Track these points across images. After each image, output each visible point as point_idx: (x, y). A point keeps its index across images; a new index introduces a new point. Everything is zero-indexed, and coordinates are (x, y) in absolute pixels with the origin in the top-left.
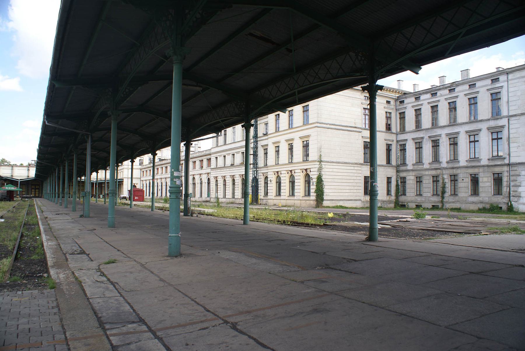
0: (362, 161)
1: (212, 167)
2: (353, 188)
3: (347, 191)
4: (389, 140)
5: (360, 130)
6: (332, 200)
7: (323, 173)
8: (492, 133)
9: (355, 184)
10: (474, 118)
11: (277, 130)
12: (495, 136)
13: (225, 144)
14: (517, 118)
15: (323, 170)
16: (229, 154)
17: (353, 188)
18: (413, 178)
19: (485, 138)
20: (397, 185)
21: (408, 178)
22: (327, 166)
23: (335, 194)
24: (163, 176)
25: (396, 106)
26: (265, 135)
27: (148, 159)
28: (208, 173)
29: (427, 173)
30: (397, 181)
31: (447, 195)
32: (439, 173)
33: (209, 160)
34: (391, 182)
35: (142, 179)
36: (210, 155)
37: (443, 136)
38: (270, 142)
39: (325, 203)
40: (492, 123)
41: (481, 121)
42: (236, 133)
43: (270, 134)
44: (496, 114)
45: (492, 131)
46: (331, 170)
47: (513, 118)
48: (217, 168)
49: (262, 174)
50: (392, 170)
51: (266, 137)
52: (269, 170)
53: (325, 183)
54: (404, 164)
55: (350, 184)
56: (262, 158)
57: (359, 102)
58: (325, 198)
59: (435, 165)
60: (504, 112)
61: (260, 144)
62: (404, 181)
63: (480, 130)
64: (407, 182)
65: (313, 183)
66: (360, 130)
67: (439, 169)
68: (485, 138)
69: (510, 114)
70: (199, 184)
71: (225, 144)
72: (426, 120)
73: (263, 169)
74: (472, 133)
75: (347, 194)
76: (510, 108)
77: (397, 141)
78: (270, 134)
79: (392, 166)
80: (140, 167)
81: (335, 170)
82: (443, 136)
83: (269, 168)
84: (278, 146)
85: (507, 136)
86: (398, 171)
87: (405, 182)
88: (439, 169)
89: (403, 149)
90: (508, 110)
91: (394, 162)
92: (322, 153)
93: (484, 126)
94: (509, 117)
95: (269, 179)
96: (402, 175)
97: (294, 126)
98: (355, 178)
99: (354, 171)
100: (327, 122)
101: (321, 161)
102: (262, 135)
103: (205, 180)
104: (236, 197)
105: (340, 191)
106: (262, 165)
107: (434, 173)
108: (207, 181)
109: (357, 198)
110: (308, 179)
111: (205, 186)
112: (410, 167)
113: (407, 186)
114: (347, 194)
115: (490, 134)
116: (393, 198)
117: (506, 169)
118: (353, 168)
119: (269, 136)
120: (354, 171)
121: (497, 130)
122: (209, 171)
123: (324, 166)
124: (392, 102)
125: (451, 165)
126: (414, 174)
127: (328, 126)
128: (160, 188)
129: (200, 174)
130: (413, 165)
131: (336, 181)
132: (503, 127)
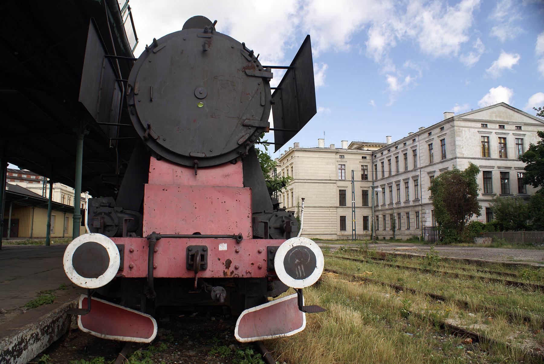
0: (338, 205)
2: (328, 225)
3: (323, 227)
4: (365, 187)
5: (335, 182)
9: (330, 222)
17: (328, 225)
23: (312, 230)
25: (372, 160)
31: (396, 229)
37: (394, 183)
46: (308, 213)
50: (369, 211)
57: (334, 161)
66: (335, 182)
75: (323, 230)
98: (331, 218)
101: (299, 207)
109: (333, 233)
114: (323, 230)
116: (370, 232)
117: (420, 208)
124: (368, 157)
127: (305, 181)
131: (313, 220)
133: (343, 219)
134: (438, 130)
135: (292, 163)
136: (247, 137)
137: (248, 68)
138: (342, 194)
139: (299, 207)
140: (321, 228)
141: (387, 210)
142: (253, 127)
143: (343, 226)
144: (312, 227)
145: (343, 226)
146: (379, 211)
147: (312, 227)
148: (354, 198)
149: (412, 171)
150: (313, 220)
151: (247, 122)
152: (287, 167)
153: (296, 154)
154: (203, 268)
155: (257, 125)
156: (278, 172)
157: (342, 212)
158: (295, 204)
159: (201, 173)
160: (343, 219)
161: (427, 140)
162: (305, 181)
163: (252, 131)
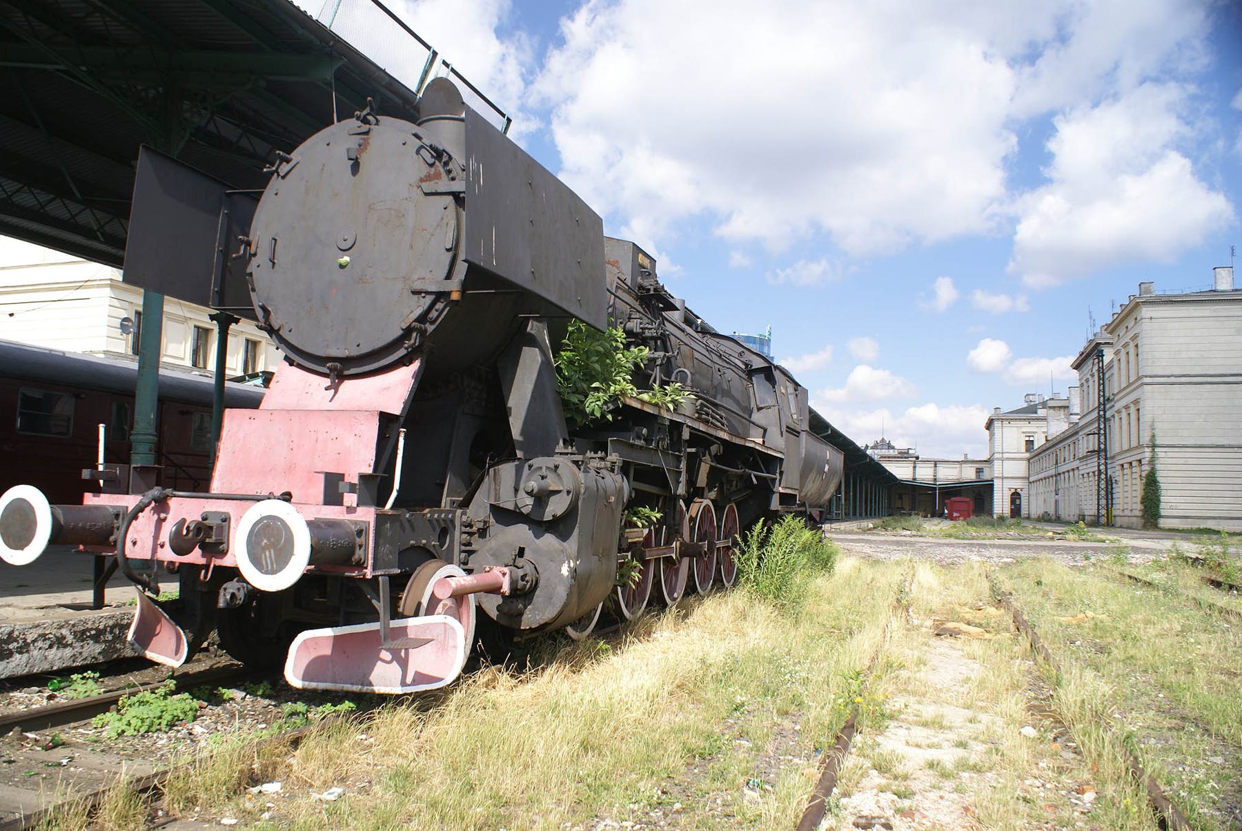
3: (1227, 500)
6: (1187, 517)
7: (1158, 467)
15: (1162, 461)
35: (1031, 479)
36: (1077, 433)
39: (1163, 523)
46: (1182, 461)
58: (1163, 512)
80: (1027, 455)
81: (1191, 461)
92: (1156, 432)
100: (1168, 373)
101: (1154, 446)
105: (1207, 500)
123: (1161, 455)
127: (1172, 380)
131: (1196, 480)
135: (1135, 337)
136: (418, 312)
137: (428, 178)
139: (1154, 446)
140: (1220, 501)
142: (427, 293)
144: (1195, 500)
147: (1195, 500)
150: (1196, 480)
151: (418, 286)
152: (1126, 345)
153: (1146, 312)
154: (224, 553)
155: (434, 289)
156: (1106, 359)
158: (1145, 440)
159: (347, 385)
163: (429, 299)
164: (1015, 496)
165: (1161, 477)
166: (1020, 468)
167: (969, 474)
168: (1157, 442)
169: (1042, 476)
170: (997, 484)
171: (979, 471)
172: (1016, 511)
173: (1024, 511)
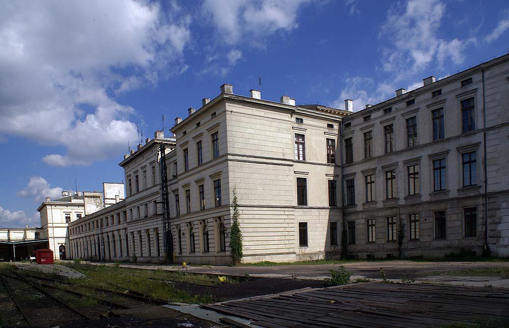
0: (295, 203)
1: (128, 220)
2: (283, 238)
5: (291, 163)
7: (239, 221)
8: (463, 155)
10: (438, 134)
11: (186, 170)
12: (467, 159)
13: (138, 192)
14: (497, 131)
15: (240, 217)
16: (142, 204)
17: (283, 238)
18: (363, 221)
19: (453, 164)
20: (344, 233)
21: (357, 222)
22: (245, 212)
24: (87, 234)
26: (175, 177)
27: (76, 216)
28: (126, 229)
29: (380, 214)
30: (344, 227)
32: (395, 213)
33: (125, 212)
34: (336, 228)
35: (70, 238)
36: (125, 206)
37: (401, 164)
38: (179, 185)
40: (463, 141)
41: (449, 139)
42: (147, 177)
43: (180, 175)
44: (468, 126)
45: (463, 151)
47: (491, 132)
48: (132, 222)
49: (175, 227)
51: (176, 180)
52: (182, 221)
53: (243, 234)
54: (352, 203)
55: (280, 234)
56: (174, 207)
59: (390, 204)
60: (479, 125)
61: (170, 189)
62: (352, 225)
63: (447, 152)
64: (357, 227)
65: (227, 234)
66: (291, 163)
67: (395, 207)
68: (453, 164)
69: (487, 127)
70: (119, 241)
71: (138, 192)
72: (378, 148)
73: (176, 220)
74: (437, 158)
76: (487, 119)
77: (343, 177)
78: (180, 175)
79: (338, 208)
82: (401, 164)
83: (181, 218)
84: (189, 190)
85: (483, 157)
86: (344, 215)
87: (354, 227)
88: (395, 207)
89: (351, 185)
90: (485, 121)
91: (339, 204)
92: (237, 196)
93: (452, 146)
94: (486, 130)
95: (182, 232)
96: (351, 218)
97: (204, 161)
99: (284, 217)
101: (236, 206)
102: (172, 178)
103: (123, 237)
104: (152, 255)
106: (175, 215)
107: (389, 213)
108: (125, 238)
110: (222, 232)
111: (124, 242)
112: (360, 208)
113: (357, 232)
115: (461, 156)
118: (282, 213)
119: (179, 178)
120: (284, 217)
121: (470, 150)
122: (125, 225)
123: (240, 212)
125: (410, 202)
126: (364, 217)
127: (245, 158)
128: (86, 247)
129: (119, 230)
130: (363, 204)
132: (477, 145)
133: (303, 227)
134: (381, 113)
138: (302, 185)
139: (236, 206)
141: (380, 209)
143: (303, 241)
145: (303, 241)
146: (357, 212)
148: (318, 194)
149: (402, 152)
150: (260, 230)
157: (301, 215)
160: (303, 227)
161: (458, 93)
162: (245, 158)
164: (62, 248)
165: (242, 227)
166: (63, 232)
167: (31, 236)
168: (238, 203)
169: (83, 235)
170: (51, 241)
171: (37, 234)
172: (63, 256)
173: (68, 256)
